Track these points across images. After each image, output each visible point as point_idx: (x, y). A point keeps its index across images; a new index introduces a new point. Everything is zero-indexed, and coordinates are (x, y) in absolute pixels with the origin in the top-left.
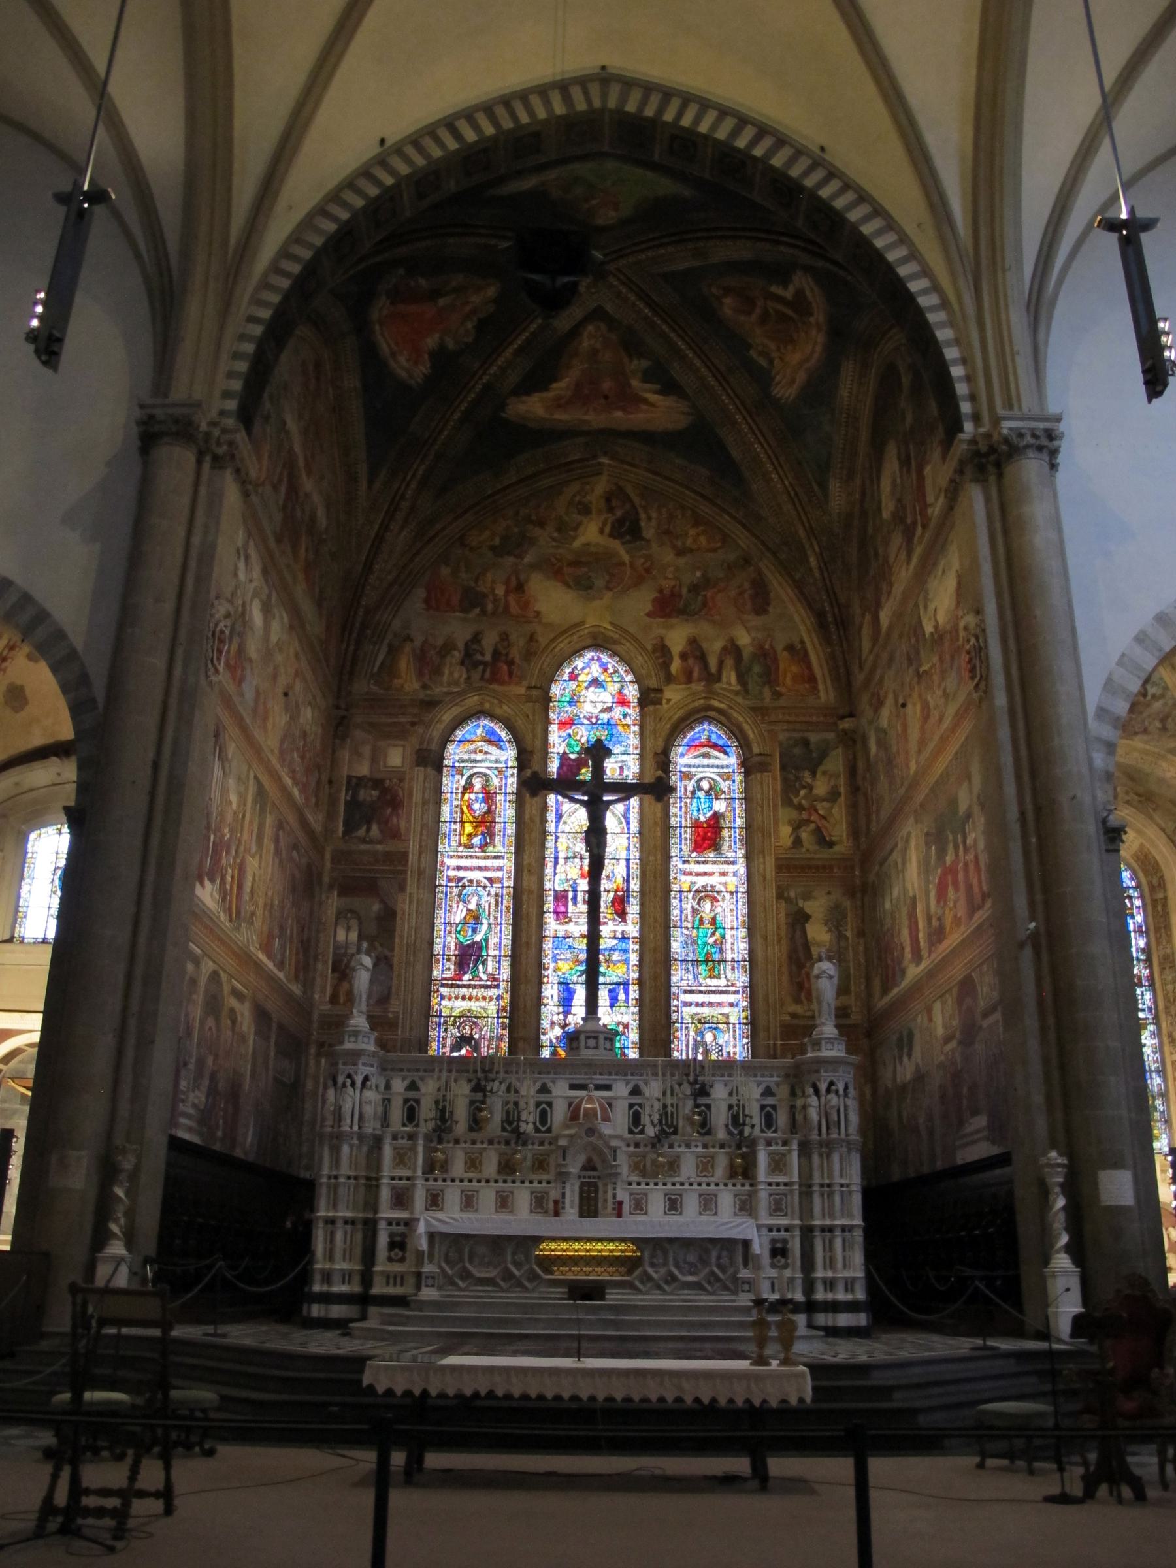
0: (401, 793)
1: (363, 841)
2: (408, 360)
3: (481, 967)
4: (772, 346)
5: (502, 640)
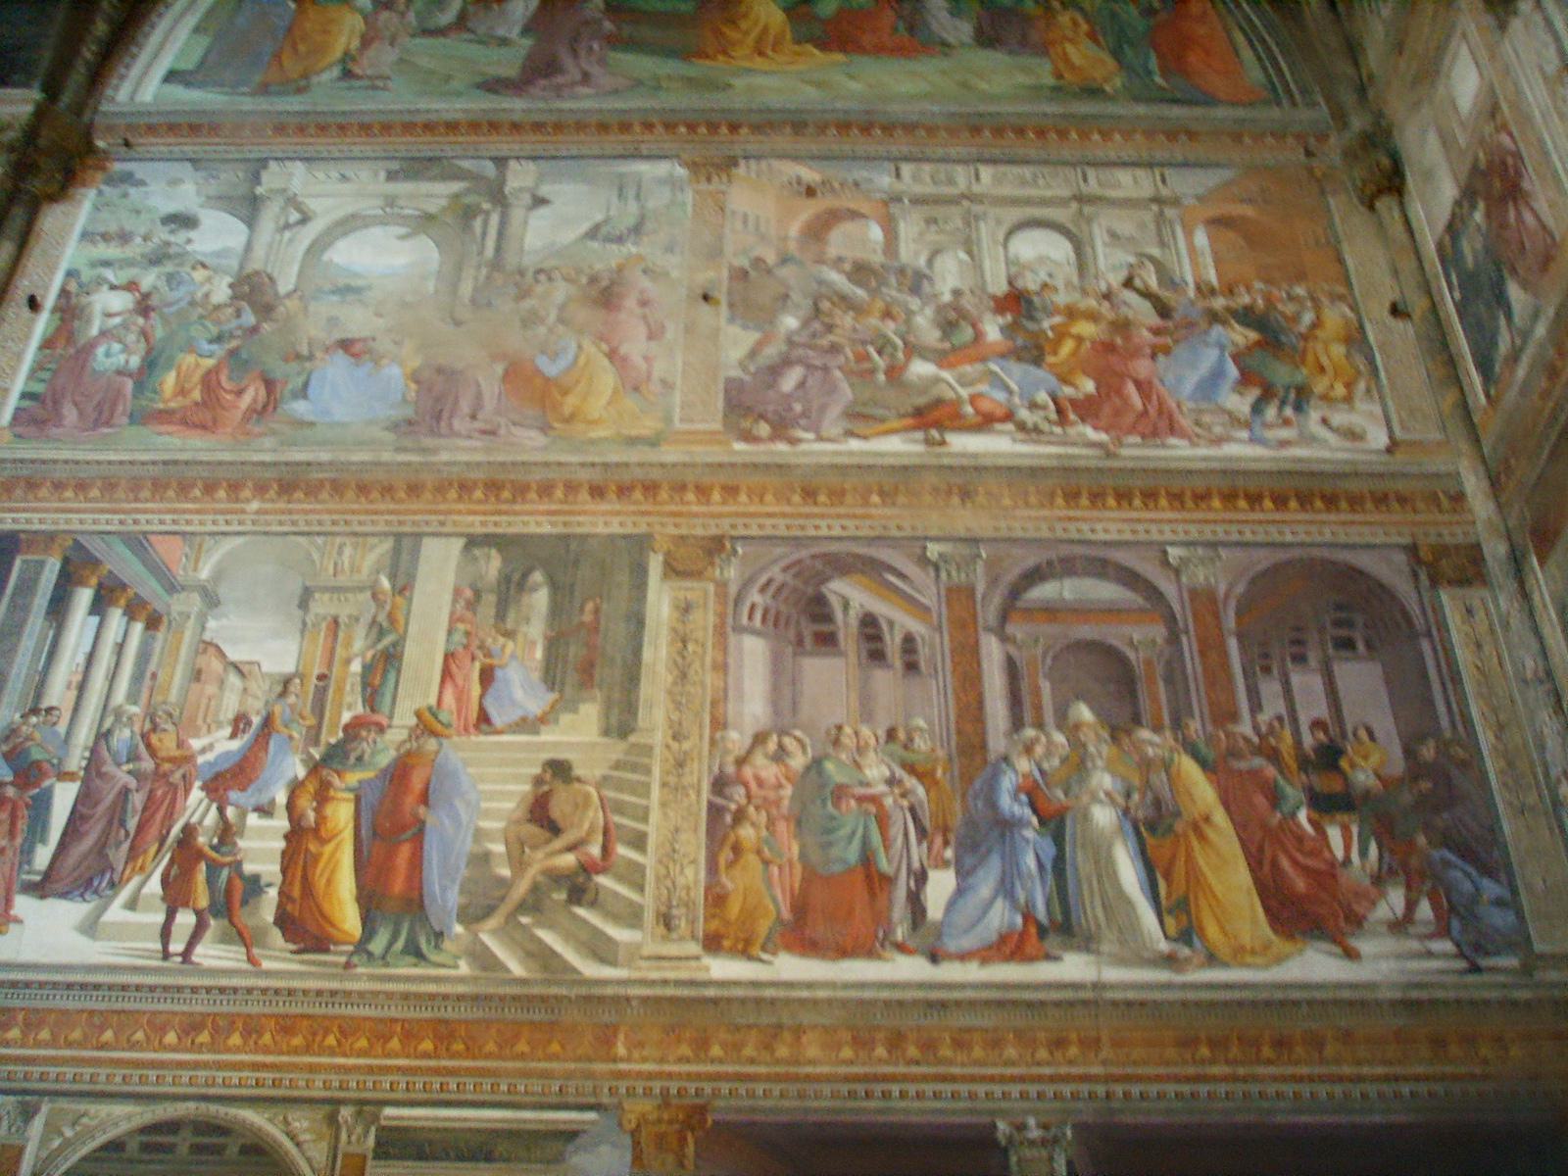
0: (1505, 140)
1: (1514, 358)
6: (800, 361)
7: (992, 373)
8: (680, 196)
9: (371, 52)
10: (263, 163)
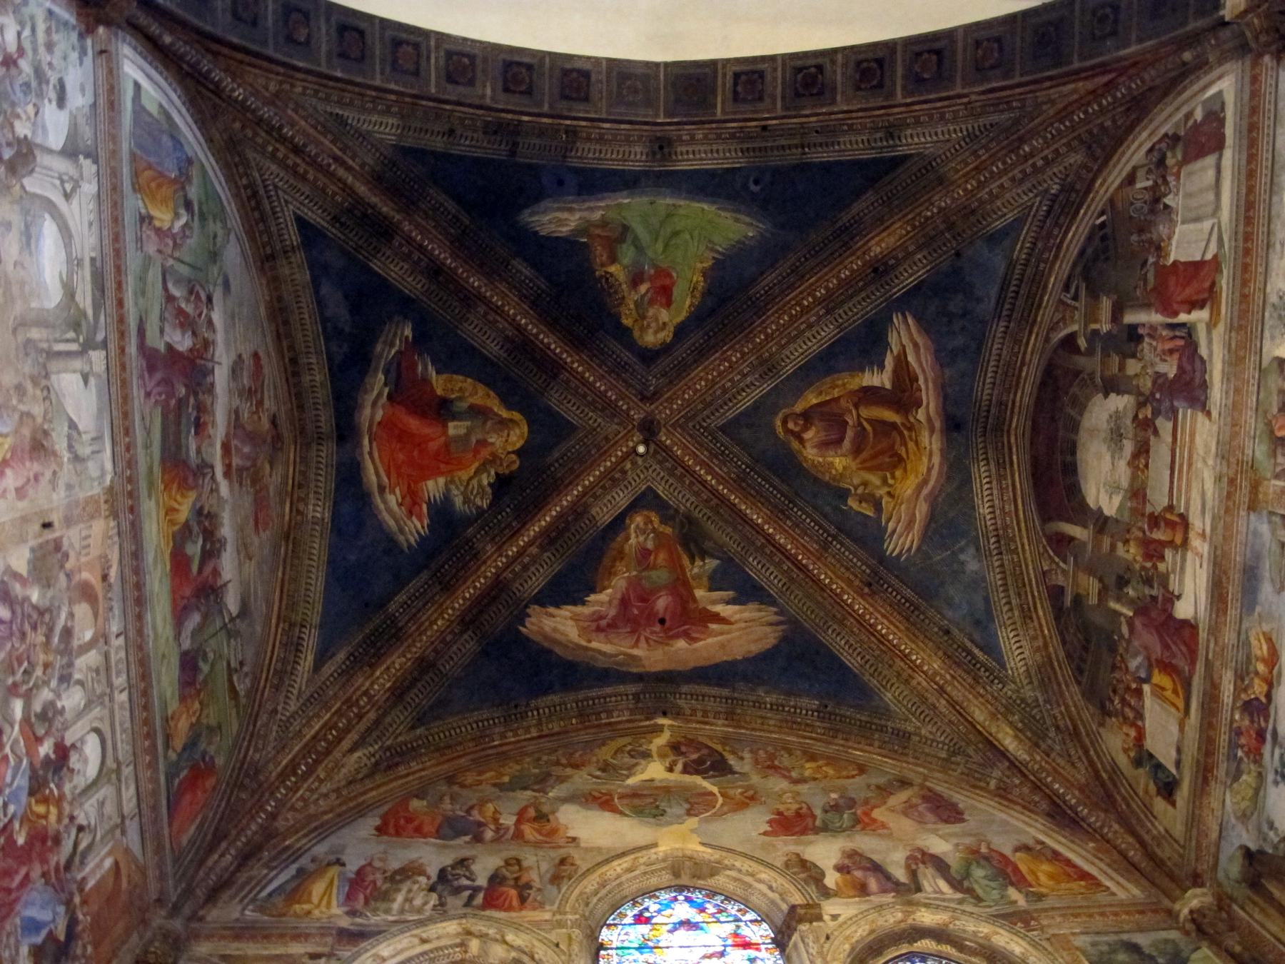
2: (400, 505)
4: (874, 479)
5: (507, 863)
6: (13, 612)
7: (21, 761)
8: (96, 483)
9: (152, 234)
10: (96, 162)
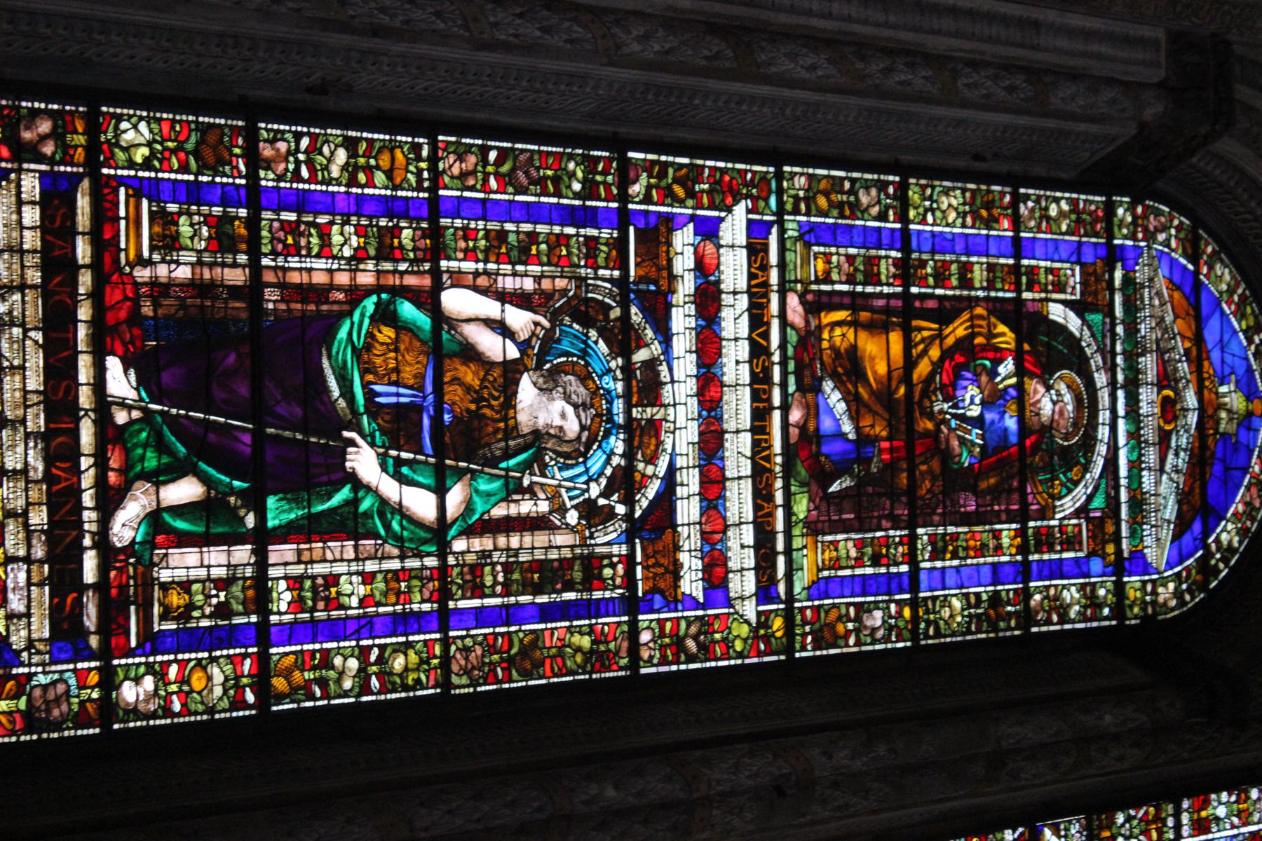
3: (185, 491)
